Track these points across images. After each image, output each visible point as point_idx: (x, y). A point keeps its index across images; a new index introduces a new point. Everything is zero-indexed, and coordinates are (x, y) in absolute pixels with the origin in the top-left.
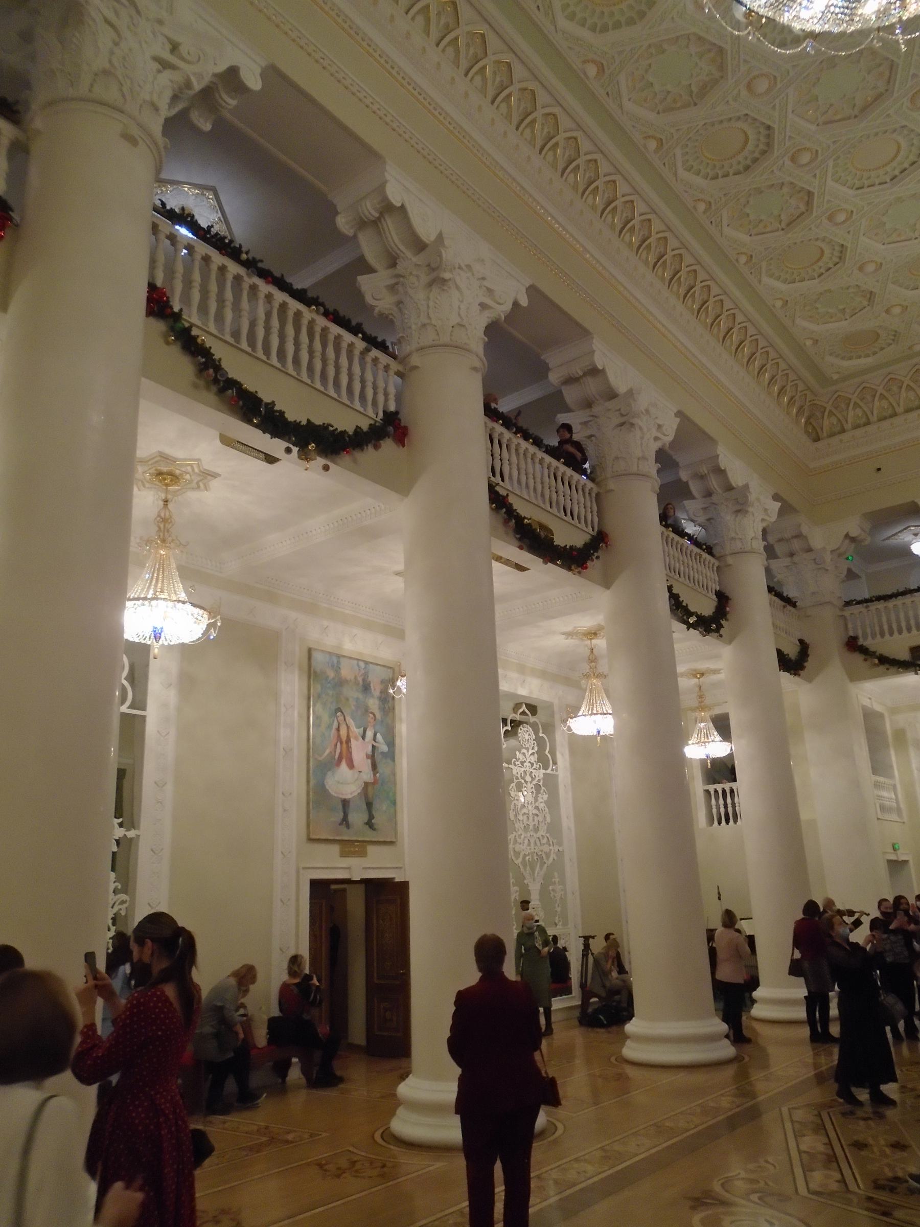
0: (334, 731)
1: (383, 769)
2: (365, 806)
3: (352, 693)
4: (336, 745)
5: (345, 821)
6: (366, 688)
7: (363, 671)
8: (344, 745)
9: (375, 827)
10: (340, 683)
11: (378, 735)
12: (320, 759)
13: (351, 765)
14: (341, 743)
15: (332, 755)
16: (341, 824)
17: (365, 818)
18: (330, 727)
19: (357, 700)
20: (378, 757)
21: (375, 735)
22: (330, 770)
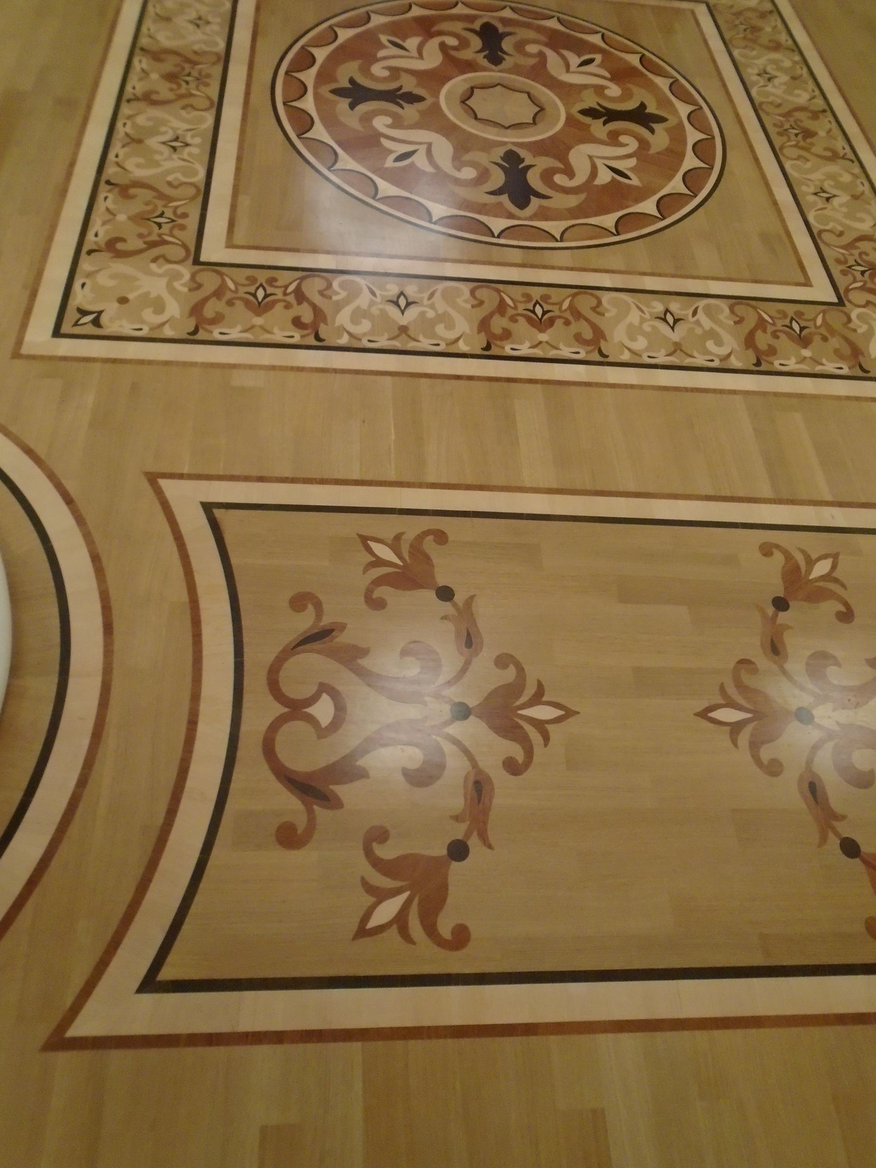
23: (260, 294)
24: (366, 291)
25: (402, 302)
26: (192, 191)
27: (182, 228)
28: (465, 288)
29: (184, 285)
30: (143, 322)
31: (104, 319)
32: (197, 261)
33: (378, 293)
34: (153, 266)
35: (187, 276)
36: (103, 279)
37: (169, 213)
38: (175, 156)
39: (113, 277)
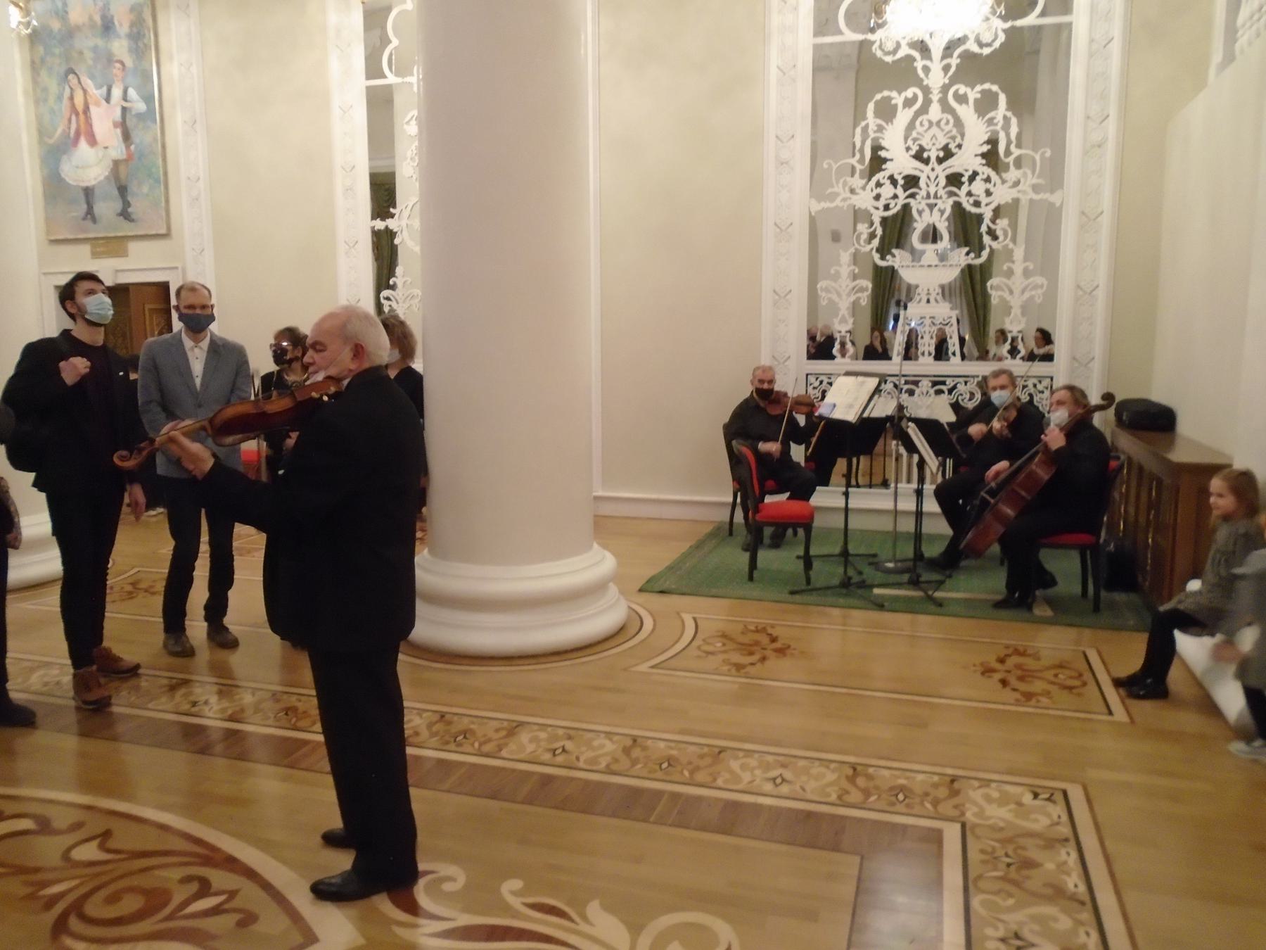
2: (116, 192)
3: (87, 43)
4: (70, 120)
5: (90, 214)
6: (107, 27)
8: (82, 117)
9: (133, 216)
10: (70, 33)
11: (132, 93)
12: (51, 141)
13: (93, 142)
14: (77, 114)
15: (66, 134)
16: (84, 219)
17: (118, 206)
18: (60, 98)
19: (95, 49)
20: (131, 123)
21: (125, 92)
22: (65, 152)
23: (901, 797)
24: (808, 788)
25: (779, 781)
26: (981, 884)
27: (983, 851)
28: (720, 782)
30: (1000, 791)
31: (1030, 796)
32: (963, 826)
33: (798, 788)
34: (1002, 824)
37: (1003, 866)
38: (1014, 927)
39: (1036, 821)
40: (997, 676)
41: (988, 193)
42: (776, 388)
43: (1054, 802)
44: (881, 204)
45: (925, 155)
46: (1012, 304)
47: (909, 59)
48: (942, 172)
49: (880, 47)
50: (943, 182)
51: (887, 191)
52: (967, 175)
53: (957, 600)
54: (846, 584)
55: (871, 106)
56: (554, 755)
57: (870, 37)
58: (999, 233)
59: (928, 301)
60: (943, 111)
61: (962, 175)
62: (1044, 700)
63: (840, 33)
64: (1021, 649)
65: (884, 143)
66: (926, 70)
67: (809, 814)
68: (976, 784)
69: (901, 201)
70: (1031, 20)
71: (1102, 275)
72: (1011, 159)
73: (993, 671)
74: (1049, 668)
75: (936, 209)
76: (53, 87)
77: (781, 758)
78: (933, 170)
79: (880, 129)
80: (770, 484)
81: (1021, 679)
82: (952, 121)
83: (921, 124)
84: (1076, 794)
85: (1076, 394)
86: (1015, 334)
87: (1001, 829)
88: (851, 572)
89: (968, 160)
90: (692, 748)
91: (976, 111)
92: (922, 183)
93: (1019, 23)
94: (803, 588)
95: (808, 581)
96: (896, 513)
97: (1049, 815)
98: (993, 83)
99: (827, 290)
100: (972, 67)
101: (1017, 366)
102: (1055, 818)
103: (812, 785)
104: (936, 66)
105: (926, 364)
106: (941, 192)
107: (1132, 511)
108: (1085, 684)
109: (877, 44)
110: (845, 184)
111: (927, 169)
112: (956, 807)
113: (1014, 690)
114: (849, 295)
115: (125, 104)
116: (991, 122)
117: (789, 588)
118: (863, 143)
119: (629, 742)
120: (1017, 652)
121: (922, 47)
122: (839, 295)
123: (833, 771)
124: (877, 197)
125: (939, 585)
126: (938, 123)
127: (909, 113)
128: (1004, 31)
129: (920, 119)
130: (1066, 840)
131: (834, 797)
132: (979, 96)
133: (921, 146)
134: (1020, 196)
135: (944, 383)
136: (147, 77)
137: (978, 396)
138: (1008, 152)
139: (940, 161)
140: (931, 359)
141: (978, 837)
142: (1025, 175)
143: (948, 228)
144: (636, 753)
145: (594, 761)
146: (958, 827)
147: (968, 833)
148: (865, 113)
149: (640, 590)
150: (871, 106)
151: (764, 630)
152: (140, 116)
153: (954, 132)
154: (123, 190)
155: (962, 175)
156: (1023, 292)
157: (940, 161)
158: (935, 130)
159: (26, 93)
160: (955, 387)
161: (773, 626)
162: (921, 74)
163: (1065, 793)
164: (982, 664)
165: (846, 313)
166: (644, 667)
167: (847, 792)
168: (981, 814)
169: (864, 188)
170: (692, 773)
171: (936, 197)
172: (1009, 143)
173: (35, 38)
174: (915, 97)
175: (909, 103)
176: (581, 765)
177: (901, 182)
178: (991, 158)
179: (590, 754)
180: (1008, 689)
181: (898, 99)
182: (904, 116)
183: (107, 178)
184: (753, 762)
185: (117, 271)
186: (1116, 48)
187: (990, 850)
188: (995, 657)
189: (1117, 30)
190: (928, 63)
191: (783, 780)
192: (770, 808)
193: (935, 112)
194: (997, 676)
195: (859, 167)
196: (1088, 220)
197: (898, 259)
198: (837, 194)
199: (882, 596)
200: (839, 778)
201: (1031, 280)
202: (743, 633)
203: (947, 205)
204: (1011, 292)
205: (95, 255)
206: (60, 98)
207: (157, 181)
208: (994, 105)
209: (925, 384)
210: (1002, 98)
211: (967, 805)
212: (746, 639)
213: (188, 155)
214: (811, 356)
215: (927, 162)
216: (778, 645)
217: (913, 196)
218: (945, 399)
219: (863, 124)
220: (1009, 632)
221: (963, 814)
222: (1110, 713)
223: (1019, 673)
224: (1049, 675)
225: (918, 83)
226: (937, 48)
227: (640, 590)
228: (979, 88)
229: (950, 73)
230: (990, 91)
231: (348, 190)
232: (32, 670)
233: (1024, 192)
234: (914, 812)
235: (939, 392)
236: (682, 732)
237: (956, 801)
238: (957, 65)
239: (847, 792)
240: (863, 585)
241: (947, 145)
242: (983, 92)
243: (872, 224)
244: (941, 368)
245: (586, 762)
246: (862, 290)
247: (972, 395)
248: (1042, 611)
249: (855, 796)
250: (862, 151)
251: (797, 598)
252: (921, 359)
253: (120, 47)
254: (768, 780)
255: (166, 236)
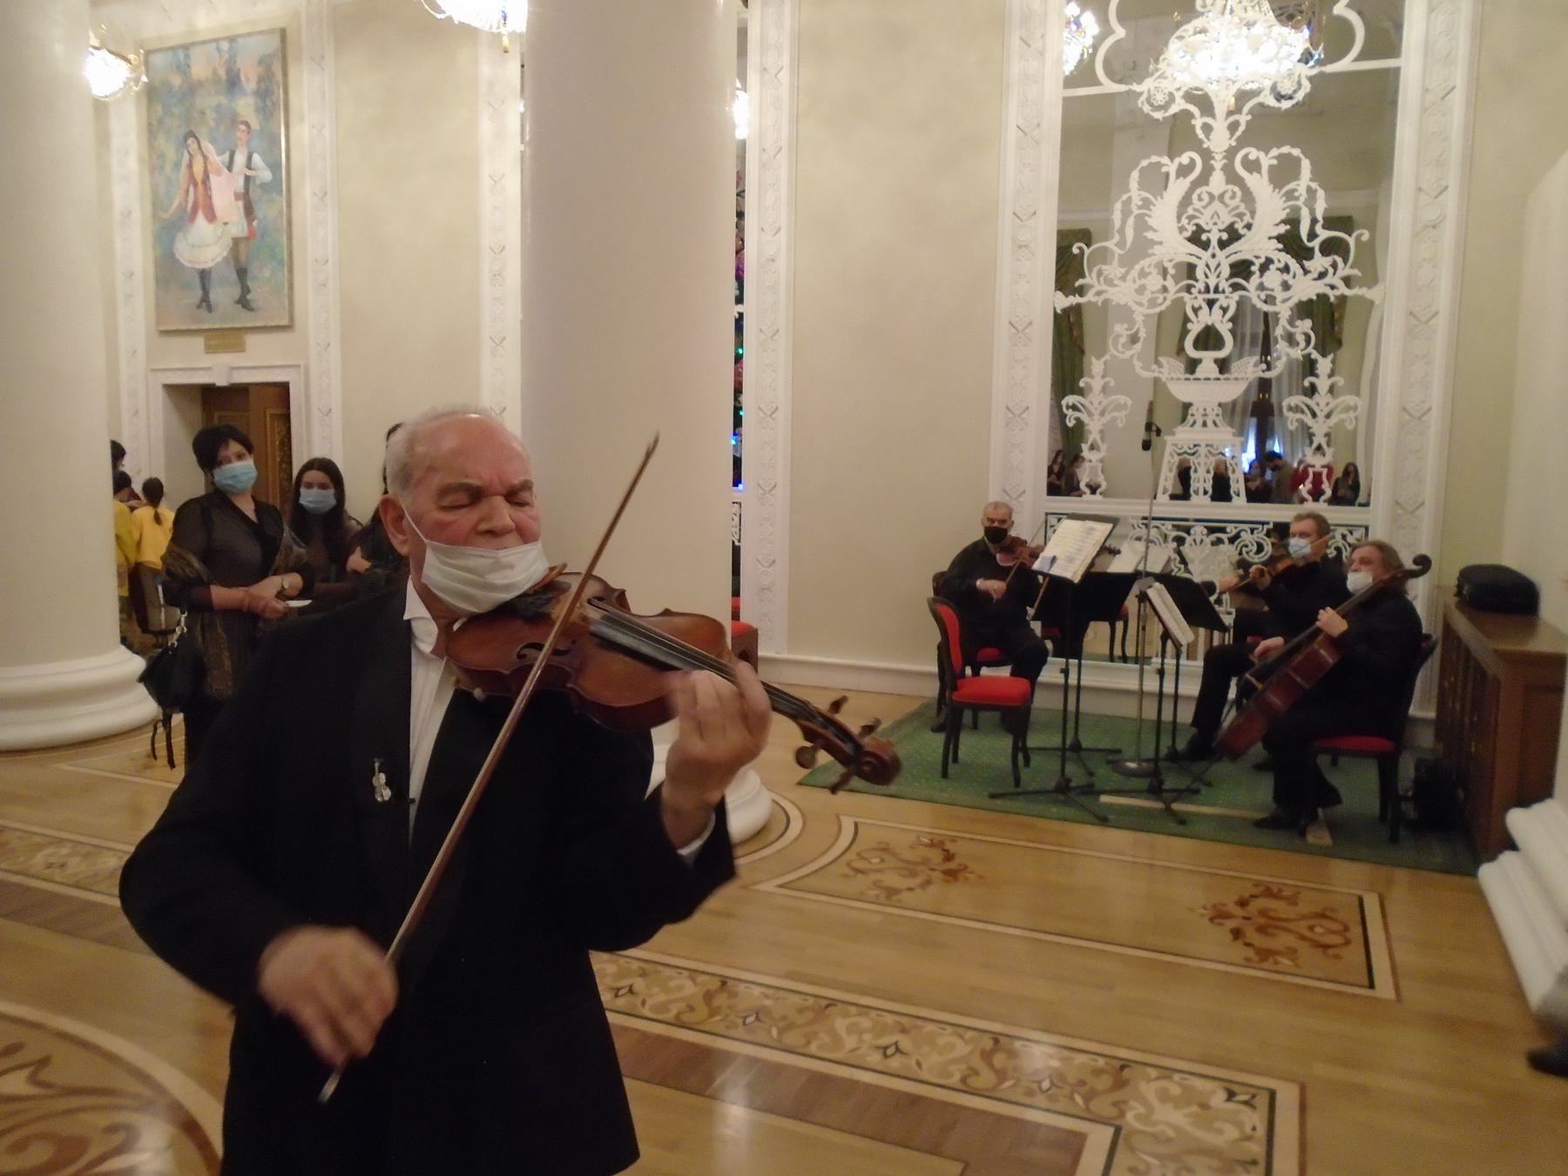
0: (184, 168)
1: (266, 211)
2: (234, 277)
3: (209, 101)
5: (205, 302)
6: (232, 83)
7: (226, 56)
9: (253, 305)
11: (256, 158)
12: (166, 216)
13: (211, 216)
14: (196, 185)
15: (182, 207)
16: (199, 307)
17: (236, 292)
18: (177, 165)
19: (218, 108)
20: (255, 194)
21: (250, 158)
22: (180, 229)
24: (925, 1065)
25: (889, 1052)
28: (813, 1049)
29: (1132, 1108)
30: (1181, 1085)
31: (1222, 1095)
32: (1118, 1131)
33: (913, 1063)
34: (1171, 1133)
35: (1130, 1116)
36: (1232, 1133)
39: (1220, 1132)
40: (1231, 924)
41: (1286, 286)
42: (1013, 533)
43: (1254, 1107)
44: (1145, 299)
45: (1204, 237)
46: (1314, 430)
47: (1186, 115)
48: (1225, 259)
49: (1148, 101)
50: (1226, 271)
51: (1155, 282)
52: (1258, 262)
53: (1205, 816)
54: (1063, 789)
55: (1135, 175)
56: (617, 996)
57: (1135, 87)
58: (1300, 338)
59: (1205, 424)
60: (1228, 182)
61: (1252, 263)
62: (1285, 962)
63: (1097, 83)
64: (1275, 890)
65: (1151, 222)
66: (1207, 129)
67: (915, 1100)
68: (1153, 1073)
69: (1171, 296)
70: (1345, 64)
71: (1436, 396)
72: (1316, 244)
73: (1227, 916)
74: (1304, 917)
75: (1216, 307)
76: (171, 152)
77: (905, 1020)
78: (1214, 256)
79: (1146, 204)
80: (990, 652)
81: (1262, 930)
82: (1239, 194)
83: (1200, 199)
84: (1288, 1096)
85: (1385, 552)
86: (1318, 469)
87: (1169, 1140)
88: (1071, 769)
89: (1259, 243)
90: (795, 999)
91: (1271, 180)
92: (1199, 273)
93: (1330, 68)
94: (1011, 789)
95: (1017, 782)
96: (1141, 694)
97: (1239, 1125)
98: (1293, 146)
99: (1074, 408)
100: (1265, 123)
101: (1321, 507)
102: (1248, 1130)
103: (933, 1060)
104: (1220, 125)
105: (1201, 505)
106: (1224, 285)
107: (1458, 706)
108: (1347, 942)
109: (1143, 98)
110: (1100, 273)
111: (1206, 255)
112: (1115, 1104)
113: (1248, 945)
114: (1102, 414)
115: (249, 173)
116: (1290, 195)
117: (992, 790)
118: (1124, 222)
119: (716, 984)
120: (1269, 893)
121: (1204, 102)
122: (1090, 414)
123: (966, 1043)
124: (1141, 290)
125: (1190, 793)
126: (1222, 196)
127: (1185, 183)
128: (1311, 79)
129: (1198, 191)
130: (1254, 1162)
131: (955, 1080)
132: (1275, 162)
133: (1197, 225)
134: (1328, 291)
135: (1223, 530)
136: (275, 141)
137: (1268, 549)
138: (1312, 235)
139: (1223, 245)
140: (1207, 499)
141: (1132, 1149)
142: (1334, 266)
143: (1233, 332)
144: (721, 1000)
145: (663, 1007)
146: (1110, 1131)
147: (1120, 1141)
148: (1127, 184)
149: (800, 784)
150: (1135, 175)
151: (942, 843)
152: (265, 187)
153: (1242, 208)
154: (242, 273)
155: (1252, 263)
156: (1328, 416)
157: (1223, 245)
158: (1217, 205)
159: (141, 160)
160: (1237, 536)
161: (954, 839)
162: (1201, 135)
163: (1272, 1095)
164: (1214, 907)
165: (1098, 438)
166: (769, 886)
167: (977, 1073)
168: (1145, 1119)
169: (1123, 278)
170: (781, 1031)
171: (1216, 290)
172: (1314, 221)
173: (152, 94)
174: (1192, 161)
175: (1184, 171)
176: (646, 1012)
177: (1172, 271)
178: (1292, 243)
179: (662, 998)
180: (1240, 942)
181: (1171, 167)
182: (1178, 188)
183: (225, 259)
184: (865, 1023)
185: (233, 369)
186: (1458, 100)
187: (1142, 1168)
188: (1236, 898)
189: (1460, 77)
190: (1209, 120)
191: (898, 1050)
192: (868, 1086)
193: (1217, 182)
194: (1231, 924)
195: (1118, 251)
196: (1417, 323)
197: (1165, 370)
198: (1091, 286)
199: (1110, 806)
200: (972, 1052)
201: (1342, 399)
202: (912, 847)
203: (1231, 300)
204: (1314, 415)
205: (210, 349)
206: (177, 165)
207: (281, 263)
208: (1296, 176)
209: (1199, 530)
210: (1306, 165)
211: (1132, 1103)
212: (910, 855)
213: (317, 232)
214: (1053, 490)
215: (1205, 246)
216: (952, 865)
217: (1188, 289)
218: (1228, 552)
219: (1125, 197)
220: (1275, 866)
221: (1122, 1114)
222: (1372, 986)
223: (1262, 921)
224: (1302, 927)
225: (1197, 145)
226: (1223, 100)
227: (800, 784)
228: (1275, 152)
229: (1238, 133)
230: (1289, 155)
231: (497, 275)
232: (40, 847)
233: (1333, 287)
234: (1057, 1107)
235: (1219, 541)
236: (789, 976)
237: (1118, 1095)
238: (1248, 122)
239: (977, 1073)
240: (1091, 791)
241: (1232, 225)
242: (1280, 157)
243: (1132, 322)
244: (1220, 511)
245: (655, 1009)
246: (1119, 407)
247: (1260, 548)
248: (1319, 837)
249: (986, 1079)
250: (1122, 231)
251: (999, 802)
252: (1194, 498)
253: (245, 106)
254: (878, 1048)
255: (288, 328)
